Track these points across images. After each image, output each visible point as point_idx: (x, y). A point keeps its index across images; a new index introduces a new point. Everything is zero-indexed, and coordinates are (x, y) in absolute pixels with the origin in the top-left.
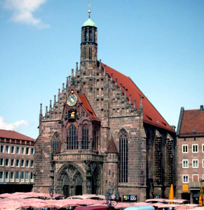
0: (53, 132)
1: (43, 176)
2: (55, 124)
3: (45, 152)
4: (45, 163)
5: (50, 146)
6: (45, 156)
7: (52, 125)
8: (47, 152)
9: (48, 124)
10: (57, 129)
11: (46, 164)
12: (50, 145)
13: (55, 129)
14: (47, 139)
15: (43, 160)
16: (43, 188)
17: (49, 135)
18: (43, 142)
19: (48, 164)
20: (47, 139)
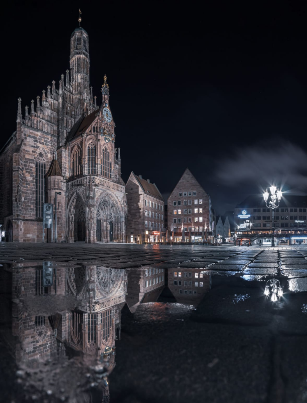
0: (39, 147)
1: (24, 205)
2: (40, 136)
3: (27, 172)
4: (27, 187)
5: (33, 165)
6: (27, 179)
7: (38, 137)
8: (29, 173)
9: (31, 133)
10: (43, 144)
11: (27, 190)
12: (34, 163)
13: (41, 143)
14: (30, 154)
15: (24, 183)
16: (24, 223)
17: (32, 149)
18: (24, 156)
19: (31, 190)
20: (30, 154)
